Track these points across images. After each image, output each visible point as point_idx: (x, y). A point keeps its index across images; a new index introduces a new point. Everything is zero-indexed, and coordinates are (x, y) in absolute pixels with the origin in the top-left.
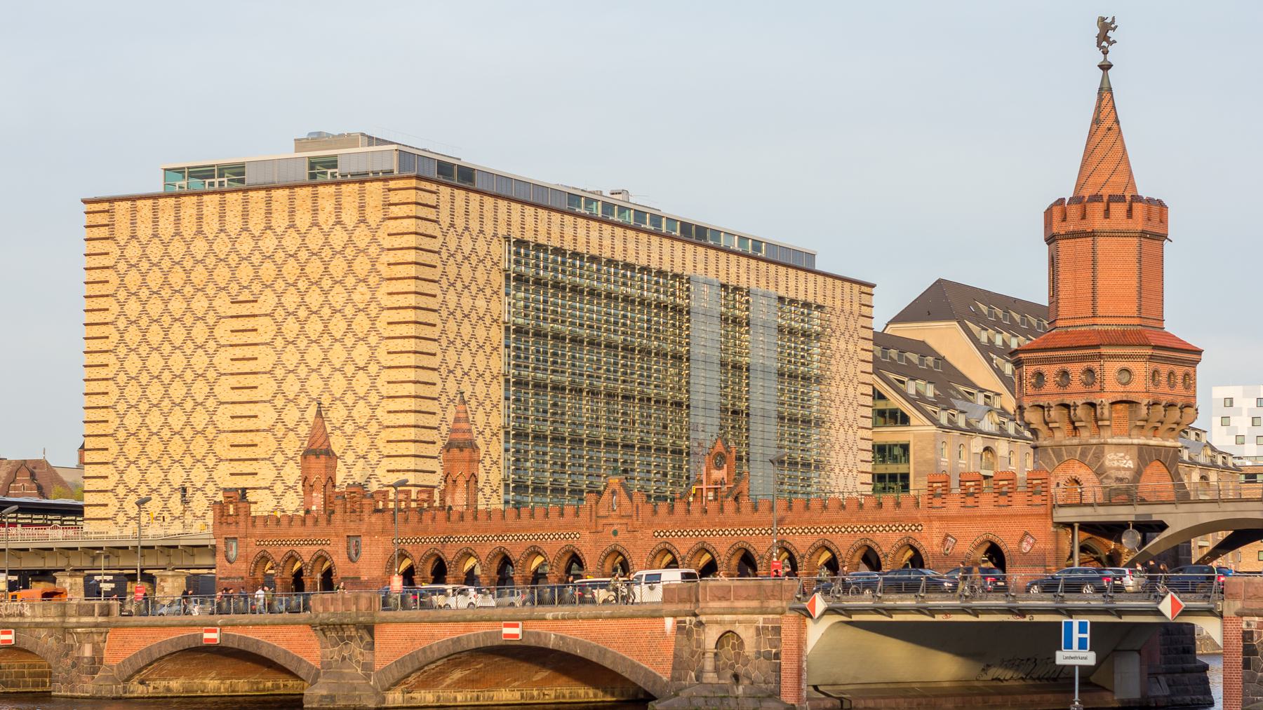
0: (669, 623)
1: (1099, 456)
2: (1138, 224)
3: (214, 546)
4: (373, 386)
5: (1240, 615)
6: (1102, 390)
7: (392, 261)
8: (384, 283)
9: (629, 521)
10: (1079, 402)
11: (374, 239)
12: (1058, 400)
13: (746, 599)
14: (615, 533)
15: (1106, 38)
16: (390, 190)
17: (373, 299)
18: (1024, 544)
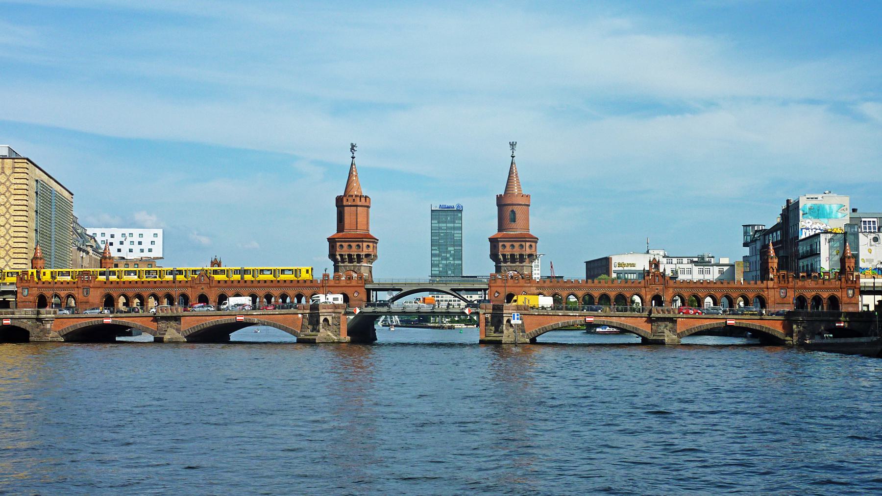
0: (300, 316)
1: (359, 269)
2: (367, 204)
3: (16, 291)
4: (7, 233)
5: (484, 314)
6: (363, 251)
7: (16, 188)
8: (13, 196)
9: (209, 285)
10: (355, 254)
11: (8, 180)
12: (348, 253)
13: (330, 309)
14: (202, 289)
15: (354, 150)
16: (15, 162)
17: (7, 201)
18: (355, 294)
